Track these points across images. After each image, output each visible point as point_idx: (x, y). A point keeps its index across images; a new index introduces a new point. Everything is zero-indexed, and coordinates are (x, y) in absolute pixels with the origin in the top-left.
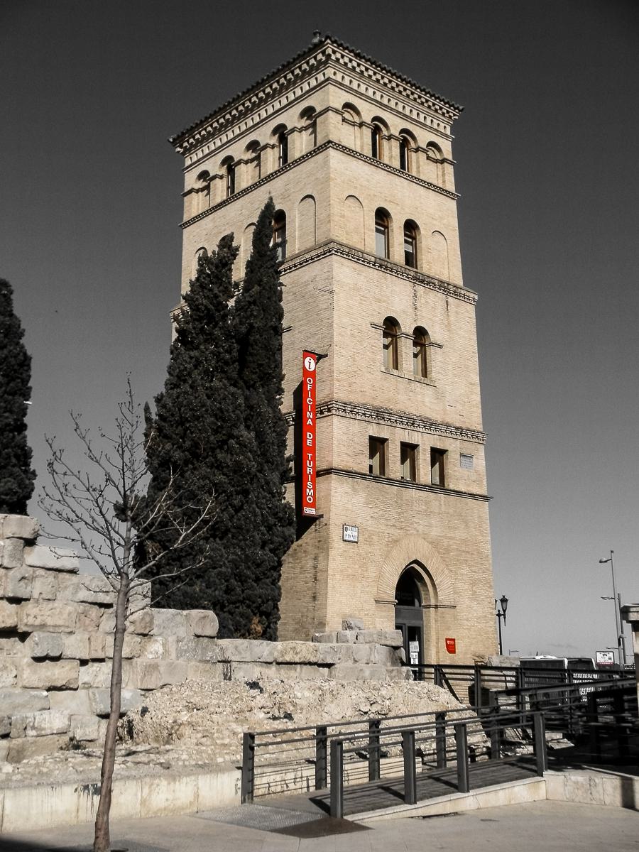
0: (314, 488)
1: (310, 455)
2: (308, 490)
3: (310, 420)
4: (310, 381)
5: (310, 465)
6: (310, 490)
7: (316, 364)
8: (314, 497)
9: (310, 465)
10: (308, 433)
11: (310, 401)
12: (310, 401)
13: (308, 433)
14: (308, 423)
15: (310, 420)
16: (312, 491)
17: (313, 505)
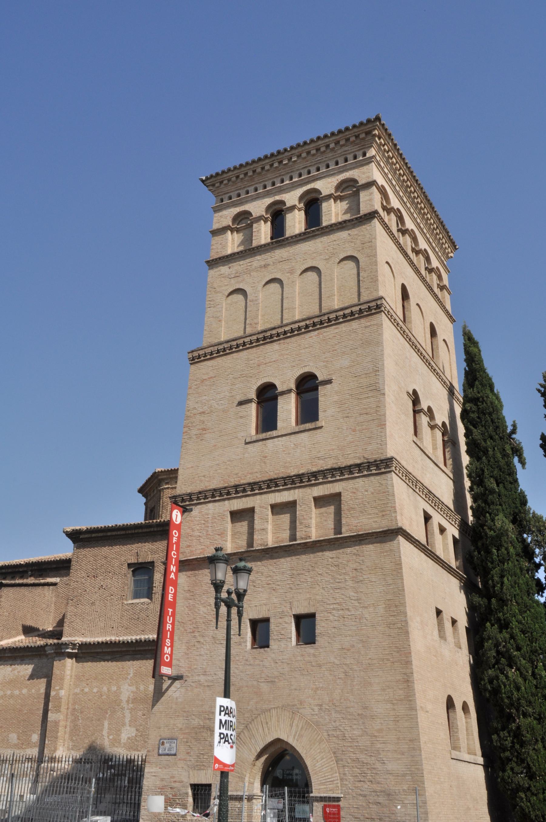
0: (172, 646)
1: (170, 610)
2: (166, 648)
3: (173, 574)
4: (175, 533)
5: (170, 620)
6: (168, 647)
7: (182, 516)
8: (171, 655)
9: (170, 620)
10: (171, 588)
11: (174, 554)
12: (174, 554)
13: (171, 588)
14: (171, 577)
15: (173, 574)
16: (170, 649)
17: (169, 665)
